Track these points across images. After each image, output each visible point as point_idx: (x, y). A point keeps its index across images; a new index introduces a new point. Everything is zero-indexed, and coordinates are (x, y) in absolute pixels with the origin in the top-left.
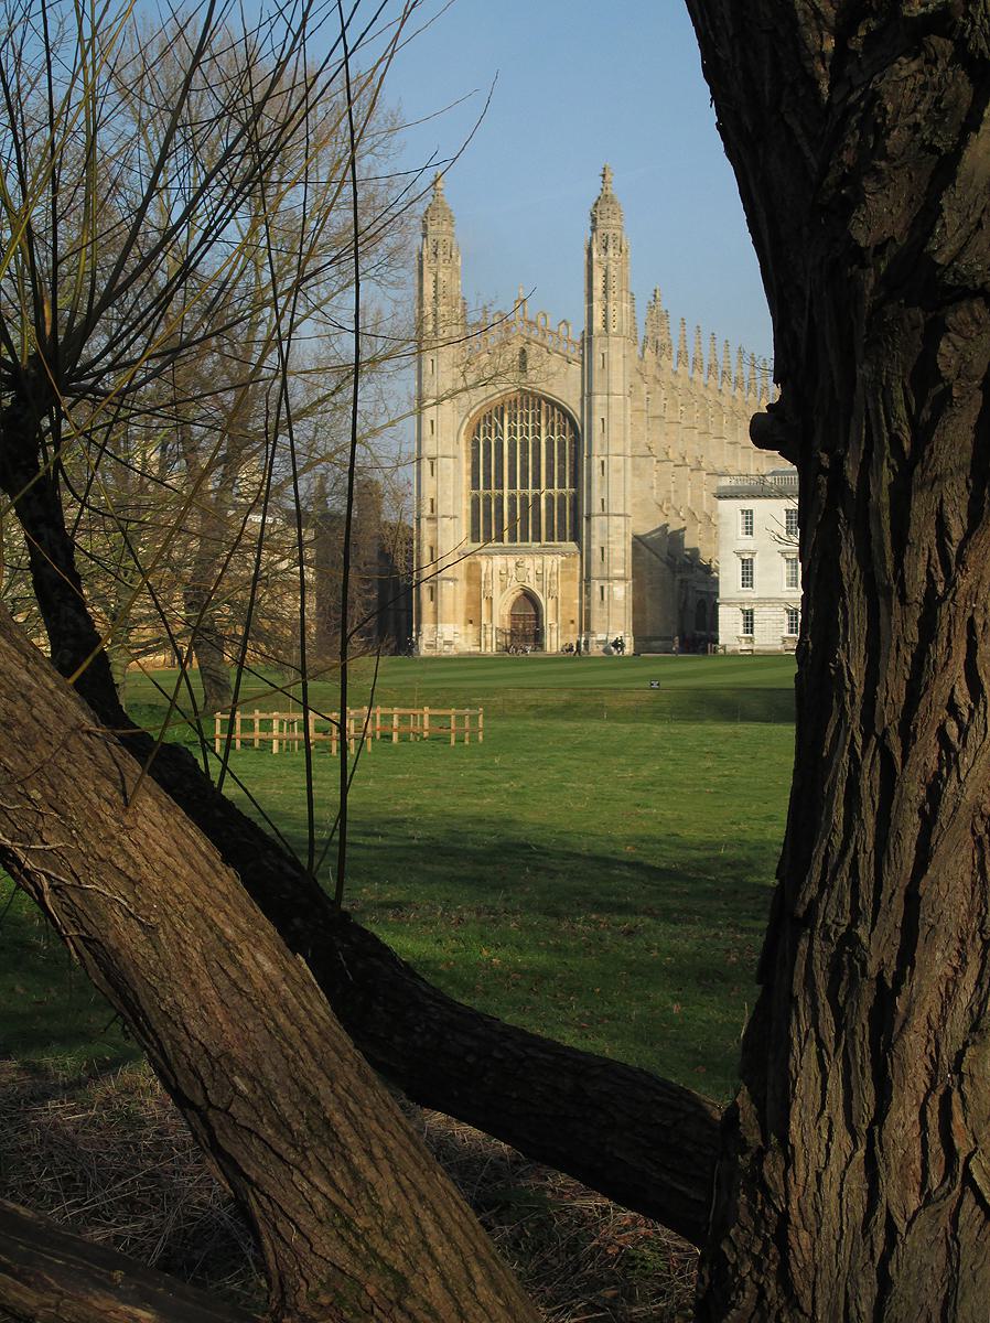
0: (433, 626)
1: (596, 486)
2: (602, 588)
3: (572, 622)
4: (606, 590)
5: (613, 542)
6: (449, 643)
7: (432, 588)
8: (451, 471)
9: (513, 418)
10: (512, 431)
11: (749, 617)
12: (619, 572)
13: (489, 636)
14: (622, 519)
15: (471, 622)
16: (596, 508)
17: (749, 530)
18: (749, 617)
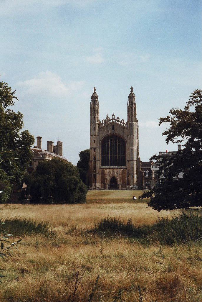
2: (132, 176)
13: (106, 186)
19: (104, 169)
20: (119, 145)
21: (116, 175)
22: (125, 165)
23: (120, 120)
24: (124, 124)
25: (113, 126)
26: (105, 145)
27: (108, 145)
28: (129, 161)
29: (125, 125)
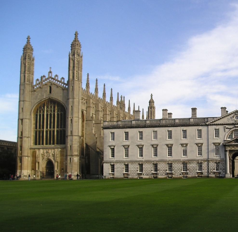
0: (20, 171)
1: (69, 126)
2: (70, 158)
3: (63, 169)
4: (71, 159)
5: (74, 144)
8: (28, 123)
9: (48, 107)
10: (47, 111)
11: (113, 167)
13: (38, 174)
14: (77, 137)
15: (33, 169)
16: (69, 134)
17: (113, 139)
18: (113, 167)
19: (36, 150)
20: (58, 114)
25: (50, 88)
27: (43, 115)
29: (66, 85)
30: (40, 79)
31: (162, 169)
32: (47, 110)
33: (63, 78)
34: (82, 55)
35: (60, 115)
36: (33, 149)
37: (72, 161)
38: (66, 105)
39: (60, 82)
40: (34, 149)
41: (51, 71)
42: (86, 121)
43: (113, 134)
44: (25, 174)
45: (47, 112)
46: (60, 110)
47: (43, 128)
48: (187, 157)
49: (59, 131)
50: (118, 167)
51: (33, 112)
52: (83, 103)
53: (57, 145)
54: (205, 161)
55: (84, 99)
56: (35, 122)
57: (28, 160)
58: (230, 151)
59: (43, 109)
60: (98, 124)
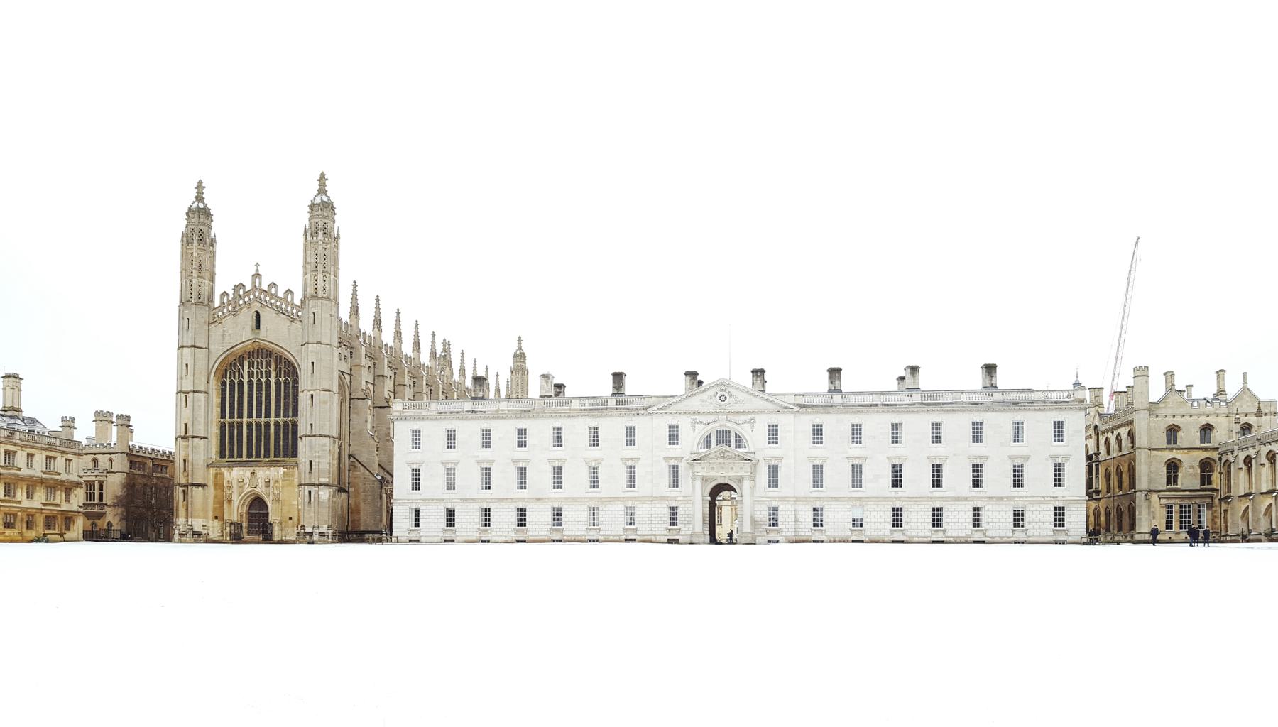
2: (310, 492)
3: (291, 518)
4: (312, 493)
5: (319, 457)
6: (199, 534)
7: (184, 491)
9: (251, 365)
10: (250, 374)
12: (325, 480)
15: (216, 518)
20: (278, 383)
21: (261, 490)
22: (295, 454)
23: (281, 294)
24: (294, 306)
25: (258, 315)
26: (232, 384)
27: (241, 384)
28: (301, 438)
30: (231, 292)
31: (536, 520)
32: (249, 372)
33: (289, 291)
34: (338, 234)
35: (282, 384)
36: (215, 468)
37: (314, 498)
38: (299, 361)
39: (284, 300)
40: (218, 469)
41: (260, 273)
42: (350, 399)
43: (417, 435)
44: (196, 529)
45: (249, 377)
46: (283, 372)
47: (240, 416)
48: (600, 492)
49: (281, 423)
50: (430, 514)
51: (214, 376)
52: (343, 358)
53: (275, 459)
54: (643, 500)
55: (344, 345)
56: (219, 400)
57: (205, 494)
58: (705, 479)
59: (241, 370)
60: (382, 410)
